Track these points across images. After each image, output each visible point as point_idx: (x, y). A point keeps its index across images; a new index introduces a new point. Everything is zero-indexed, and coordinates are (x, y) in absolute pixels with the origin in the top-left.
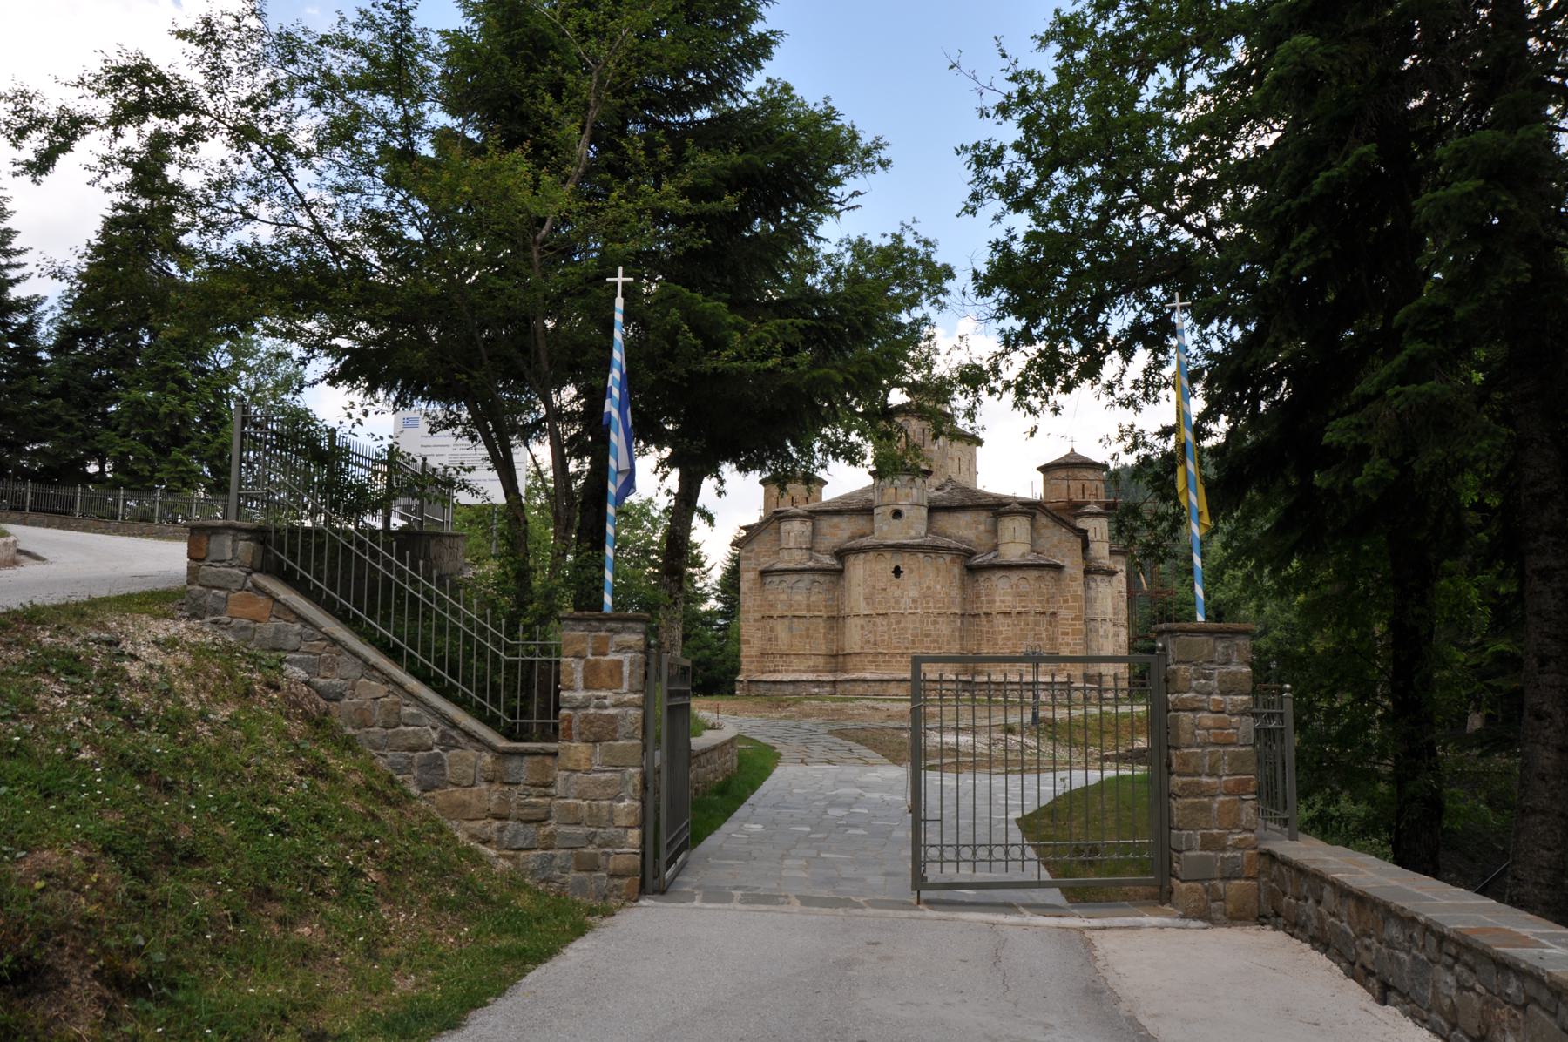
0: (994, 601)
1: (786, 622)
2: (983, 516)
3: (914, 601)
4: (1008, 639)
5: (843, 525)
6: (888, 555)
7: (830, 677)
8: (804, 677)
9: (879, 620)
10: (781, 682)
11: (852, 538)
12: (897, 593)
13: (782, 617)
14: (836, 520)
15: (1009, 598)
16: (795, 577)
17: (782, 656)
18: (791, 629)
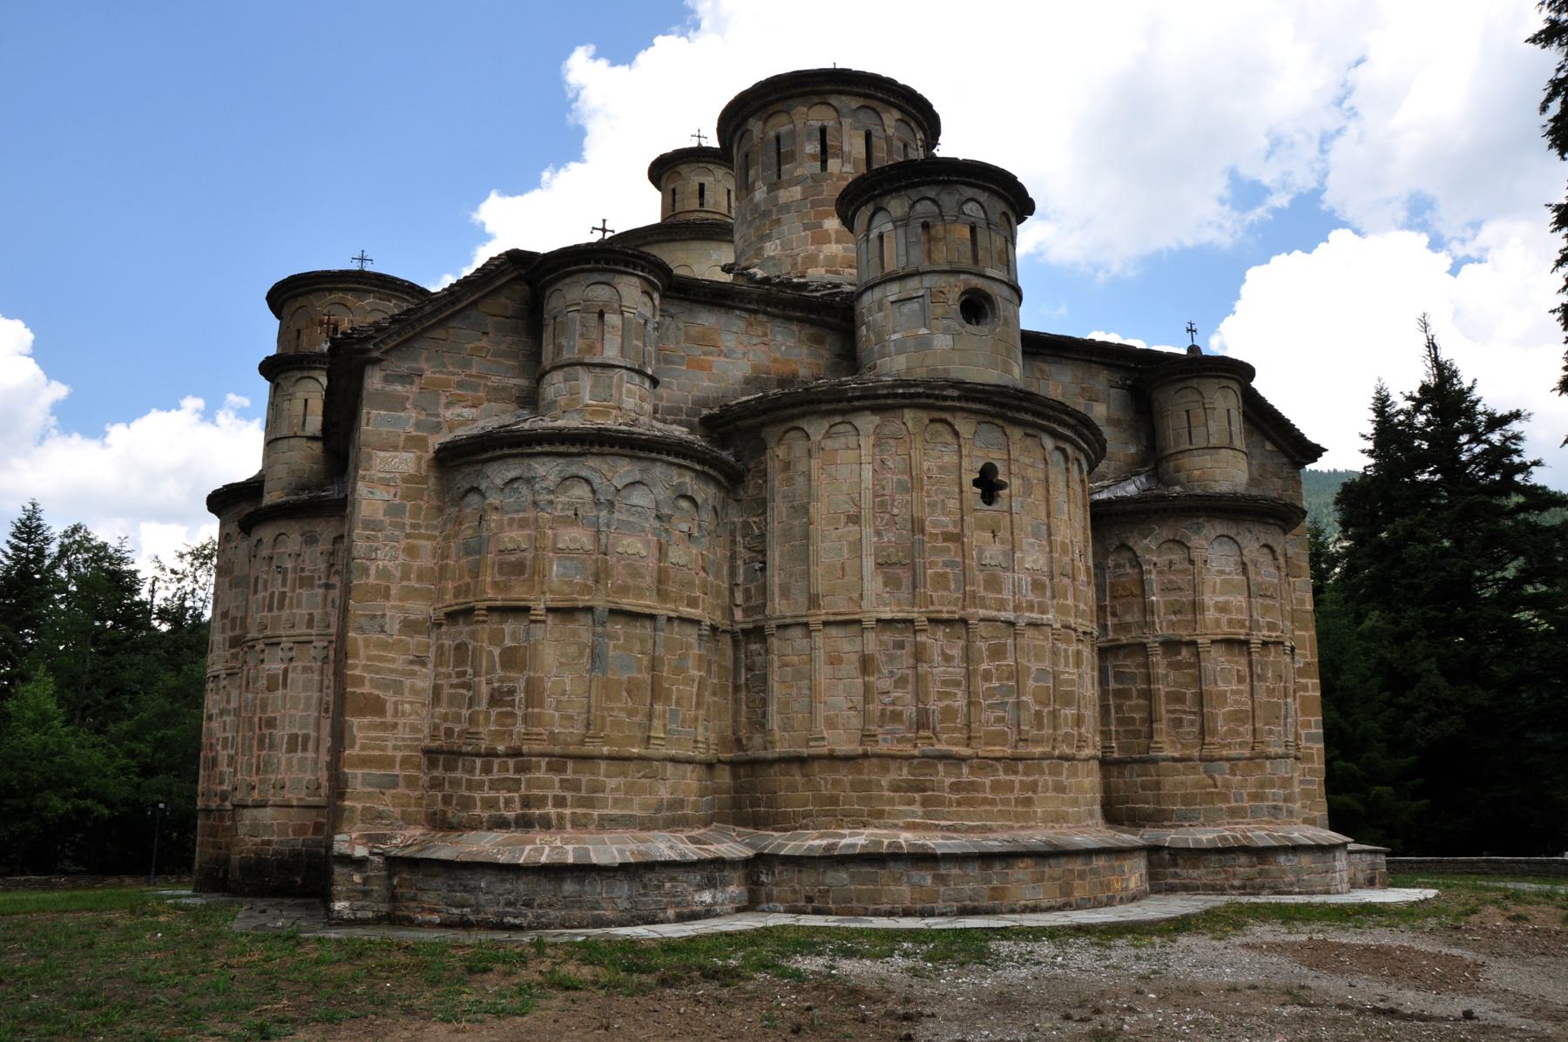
0: (1196, 607)
1: (582, 629)
5: (728, 341)
7: (731, 847)
8: (664, 846)
9: (935, 641)
10: (584, 871)
12: (994, 552)
13: (565, 612)
16: (624, 470)
17: (558, 762)
18: (597, 658)
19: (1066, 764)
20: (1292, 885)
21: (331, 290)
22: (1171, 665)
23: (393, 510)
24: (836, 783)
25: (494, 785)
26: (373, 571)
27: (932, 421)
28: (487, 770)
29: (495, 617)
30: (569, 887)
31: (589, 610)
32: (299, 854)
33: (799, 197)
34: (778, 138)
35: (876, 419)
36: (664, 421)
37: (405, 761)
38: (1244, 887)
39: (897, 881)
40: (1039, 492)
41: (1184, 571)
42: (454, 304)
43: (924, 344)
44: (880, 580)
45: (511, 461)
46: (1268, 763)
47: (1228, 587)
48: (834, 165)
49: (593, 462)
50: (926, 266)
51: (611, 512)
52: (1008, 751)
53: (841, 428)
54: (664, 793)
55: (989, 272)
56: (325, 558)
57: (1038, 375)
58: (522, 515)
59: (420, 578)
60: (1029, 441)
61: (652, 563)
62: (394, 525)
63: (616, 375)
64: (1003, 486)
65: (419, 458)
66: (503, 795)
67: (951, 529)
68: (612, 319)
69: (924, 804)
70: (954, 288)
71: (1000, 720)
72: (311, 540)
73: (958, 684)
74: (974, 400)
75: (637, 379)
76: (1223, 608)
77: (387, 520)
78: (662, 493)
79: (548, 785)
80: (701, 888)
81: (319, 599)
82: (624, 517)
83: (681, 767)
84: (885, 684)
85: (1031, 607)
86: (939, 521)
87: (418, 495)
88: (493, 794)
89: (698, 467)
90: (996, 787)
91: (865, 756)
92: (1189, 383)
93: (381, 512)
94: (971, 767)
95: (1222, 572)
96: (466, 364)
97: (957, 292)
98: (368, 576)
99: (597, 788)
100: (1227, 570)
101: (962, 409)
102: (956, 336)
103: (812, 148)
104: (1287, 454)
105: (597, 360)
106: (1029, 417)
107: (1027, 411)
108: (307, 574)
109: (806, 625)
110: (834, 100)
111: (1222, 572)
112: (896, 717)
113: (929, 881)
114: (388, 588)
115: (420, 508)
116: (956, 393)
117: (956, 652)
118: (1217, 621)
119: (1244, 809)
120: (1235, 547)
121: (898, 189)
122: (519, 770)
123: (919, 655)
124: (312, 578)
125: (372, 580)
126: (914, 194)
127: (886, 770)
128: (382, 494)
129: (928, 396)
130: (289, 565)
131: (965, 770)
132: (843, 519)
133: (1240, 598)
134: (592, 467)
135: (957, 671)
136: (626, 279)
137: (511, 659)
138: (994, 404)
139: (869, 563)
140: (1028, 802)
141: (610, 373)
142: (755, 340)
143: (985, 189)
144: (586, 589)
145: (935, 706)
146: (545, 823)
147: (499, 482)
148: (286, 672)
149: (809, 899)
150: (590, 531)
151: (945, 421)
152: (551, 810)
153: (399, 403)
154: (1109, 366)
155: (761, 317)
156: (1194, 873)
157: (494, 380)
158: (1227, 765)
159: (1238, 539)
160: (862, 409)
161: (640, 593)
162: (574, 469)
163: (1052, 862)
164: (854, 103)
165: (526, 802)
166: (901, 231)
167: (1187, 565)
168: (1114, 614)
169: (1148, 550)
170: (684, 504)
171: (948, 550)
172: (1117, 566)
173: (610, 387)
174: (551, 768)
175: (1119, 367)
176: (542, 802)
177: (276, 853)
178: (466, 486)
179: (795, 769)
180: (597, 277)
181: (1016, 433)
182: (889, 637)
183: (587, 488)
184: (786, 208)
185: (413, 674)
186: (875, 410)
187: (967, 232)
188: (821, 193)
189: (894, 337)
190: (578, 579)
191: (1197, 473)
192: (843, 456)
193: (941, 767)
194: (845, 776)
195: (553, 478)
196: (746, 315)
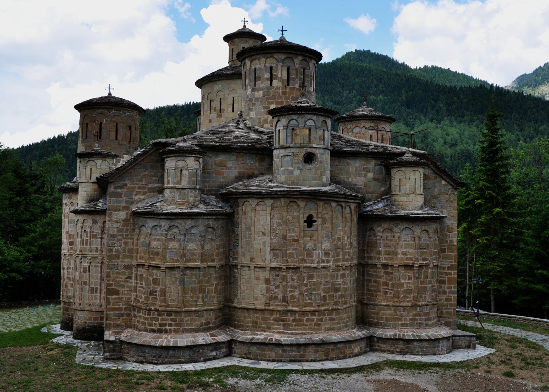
0: (396, 253)
1: (178, 274)
2: (372, 164)
3: (327, 254)
4: (409, 292)
5: (230, 164)
6: (302, 204)
7: (222, 337)
9: (290, 275)
10: (176, 348)
11: (239, 178)
12: (310, 245)
14: (222, 157)
15: (411, 250)
16: (189, 223)
18: (182, 282)
19: (335, 312)
20: (419, 352)
21: (98, 109)
22: (385, 273)
23: (120, 231)
24: (257, 317)
25: (152, 319)
26: (114, 250)
27: (290, 202)
28: (149, 314)
29: (151, 268)
30: (171, 352)
31: (179, 267)
32: (96, 326)
33: (262, 95)
34: (255, 69)
35: (272, 201)
36: (207, 195)
37: (126, 308)
38: (400, 352)
39: (271, 351)
40: (329, 222)
41: (391, 240)
42: (136, 161)
43: (291, 172)
44: (272, 254)
45: (154, 219)
46: (418, 308)
47: (407, 246)
48: (275, 82)
49: (178, 221)
50: (291, 145)
51: (185, 236)
52: (312, 309)
53: (261, 203)
54: (203, 321)
55: (315, 146)
56: (100, 229)
57: (346, 165)
58: (158, 237)
59: (129, 252)
60: (326, 205)
61: (199, 251)
62: (120, 235)
63: (186, 191)
64: (315, 221)
65: (127, 213)
66: (154, 322)
67: (296, 238)
68: (185, 172)
69: (284, 325)
70: (302, 153)
71: (310, 299)
72: (95, 222)
73: (296, 288)
74: (305, 195)
75: (194, 191)
76: (405, 254)
77: (118, 234)
78: (202, 228)
79: (167, 320)
80: (212, 351)
81: (99, 243)
82: (189, 238)
83: (209, 312)
84: (272, 287)
85: (323, 262)
86: (292, 235)
87: (127, 225)
88: (151, 322)
89: (214, 217)
90: (308, 320)
91: (265, 310)
92: (401, 169)
93: (116, 231)
94: (299, 314)
95: (406, 241)
96: (141, 181)
97: (303, 154)
98: (113, 252)
99: (182, 321)
100: (408, 240)
101: (301, 198)
102: (301, 170)
103: (267, 75)
104: (451, 185)
105: (180, 186)
106: (325, 198)
107: (324, 196)
108: (95, 234)
109: (249, 267)
110: (275, 56)
111: (406, 241)
112: (276, 298)
113: (280, 351)
114: (119, 255)
115: (128, 229)
116: (298, 193)
117: (295, 277)
118: (402, 258)
119: (407, 324)
120: (411, 231)
121: (285, 115)
122: (158, 315)
123: (284, 279)
124: (96, 235)
125: (114, 253)
126: (290, 117)
127: (272, 315)
128: (116, 225)
129: (289, 194)
130: (89, 230)
131: (297, 315)
132: (261, 234)
133: (412, 250)
134: (177, 223)
135: (296, 284)
136: (189, 158)
137: (155, 281)
138: (312, 195)
139: (268, 249)
140: (319, 325)
141: (185, 191)
142: (239, 163)
143: (315, 114)
144: (177, 261)
145: (289, 295)
146: (166, 332)
147: (151, 226)
148: (89, 267)
149: (246, 354)
150: (178, 243)
151: (295, 202)
152: (168, 328)
153: (119, 195)
154: (376, 158)
155: (242, 154)
156: (384, 346)
157: (150, 185)
158: (402, 308)
159: (413, 229)
160: (268, 198)
161: (195, 261)
162: (173, 224)
163: (322, 346)
164: (283, 57)
165: (161, 325)
166: (285, 131)
167: (392, 238)
168: (368, 253)
169: (379, 231)
170: (210, 230)
171: (294, 245)
172: (370, 236)
173: (184, 195)
174: (167, 315)
175: (380, 158)
176: (165, 325)
177: (88, 326)
178: (141, 224)
179: (246, 311)
180: (180, 158)
181: (321, 204)
182: (274, 273)
183: (177, 229)
184: (257, 99)
185: (127, 282)
186: (271, 198)
187: (307, 132)
188: (269, 95)
189: (282, 169)
190: (175, 258)
191: (401, 203)
192: (261, 213)
193: (289, 314)
194: (260, 316)
195: (167, 227)
196: (236, 154)
